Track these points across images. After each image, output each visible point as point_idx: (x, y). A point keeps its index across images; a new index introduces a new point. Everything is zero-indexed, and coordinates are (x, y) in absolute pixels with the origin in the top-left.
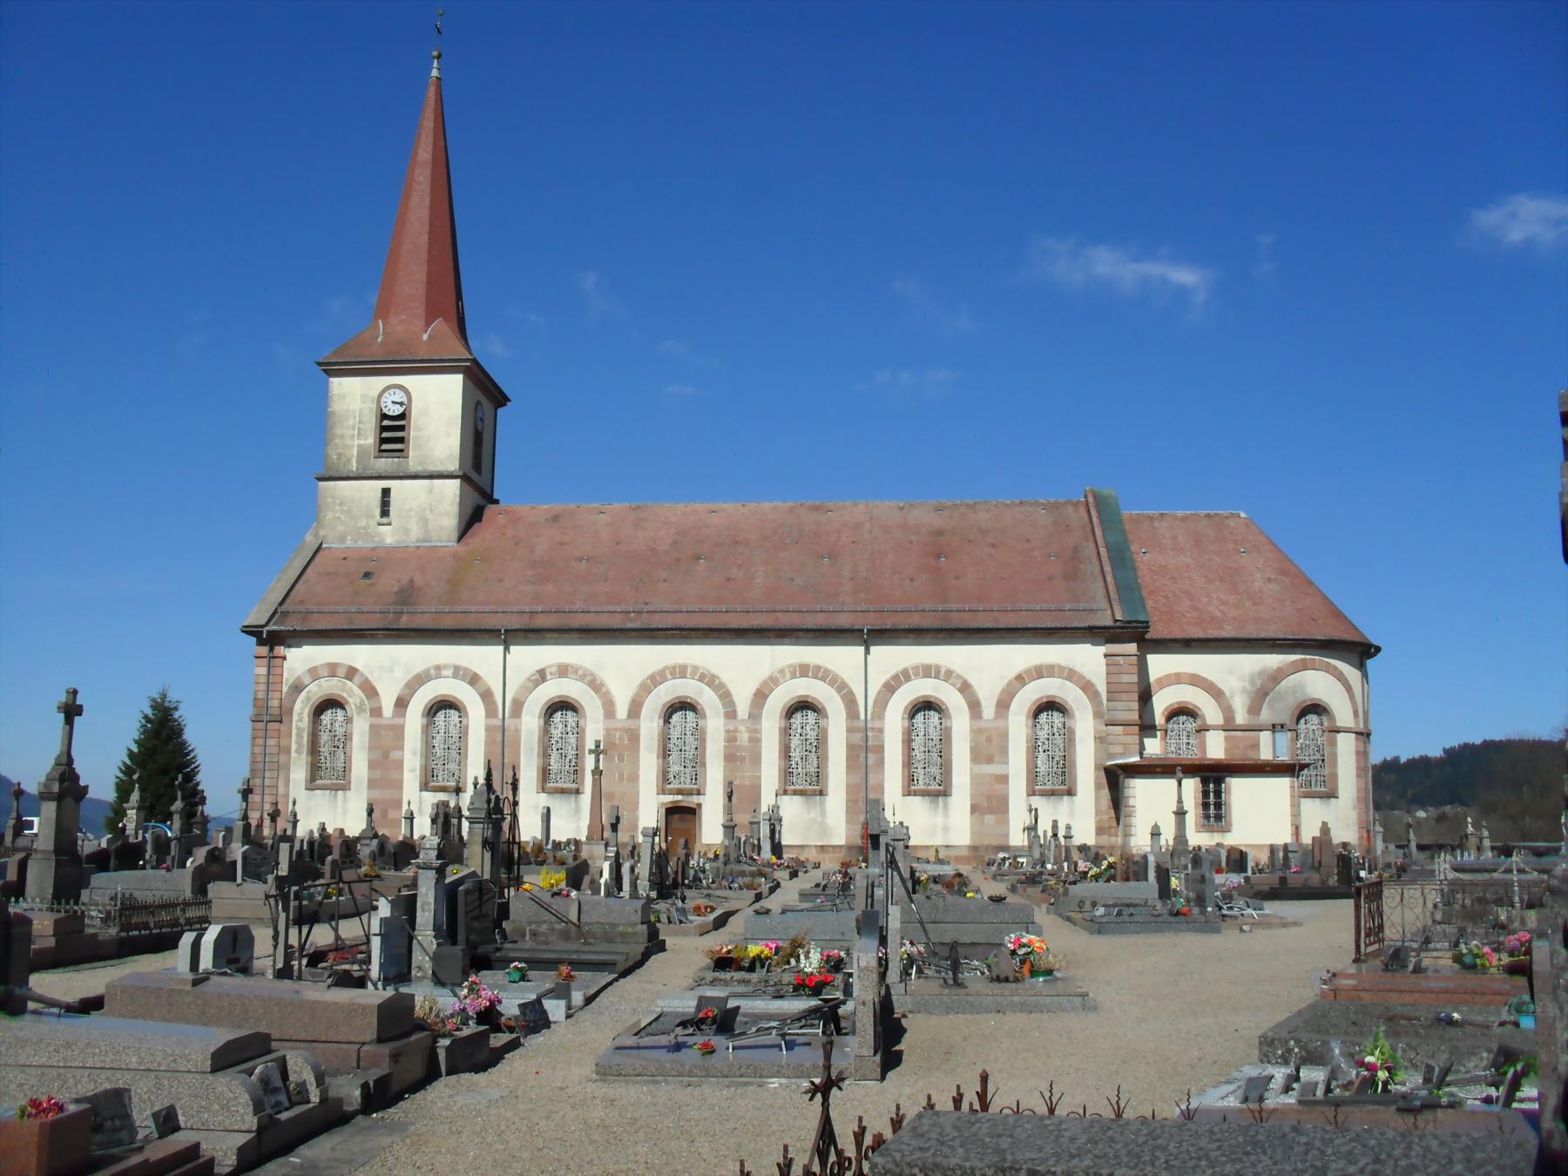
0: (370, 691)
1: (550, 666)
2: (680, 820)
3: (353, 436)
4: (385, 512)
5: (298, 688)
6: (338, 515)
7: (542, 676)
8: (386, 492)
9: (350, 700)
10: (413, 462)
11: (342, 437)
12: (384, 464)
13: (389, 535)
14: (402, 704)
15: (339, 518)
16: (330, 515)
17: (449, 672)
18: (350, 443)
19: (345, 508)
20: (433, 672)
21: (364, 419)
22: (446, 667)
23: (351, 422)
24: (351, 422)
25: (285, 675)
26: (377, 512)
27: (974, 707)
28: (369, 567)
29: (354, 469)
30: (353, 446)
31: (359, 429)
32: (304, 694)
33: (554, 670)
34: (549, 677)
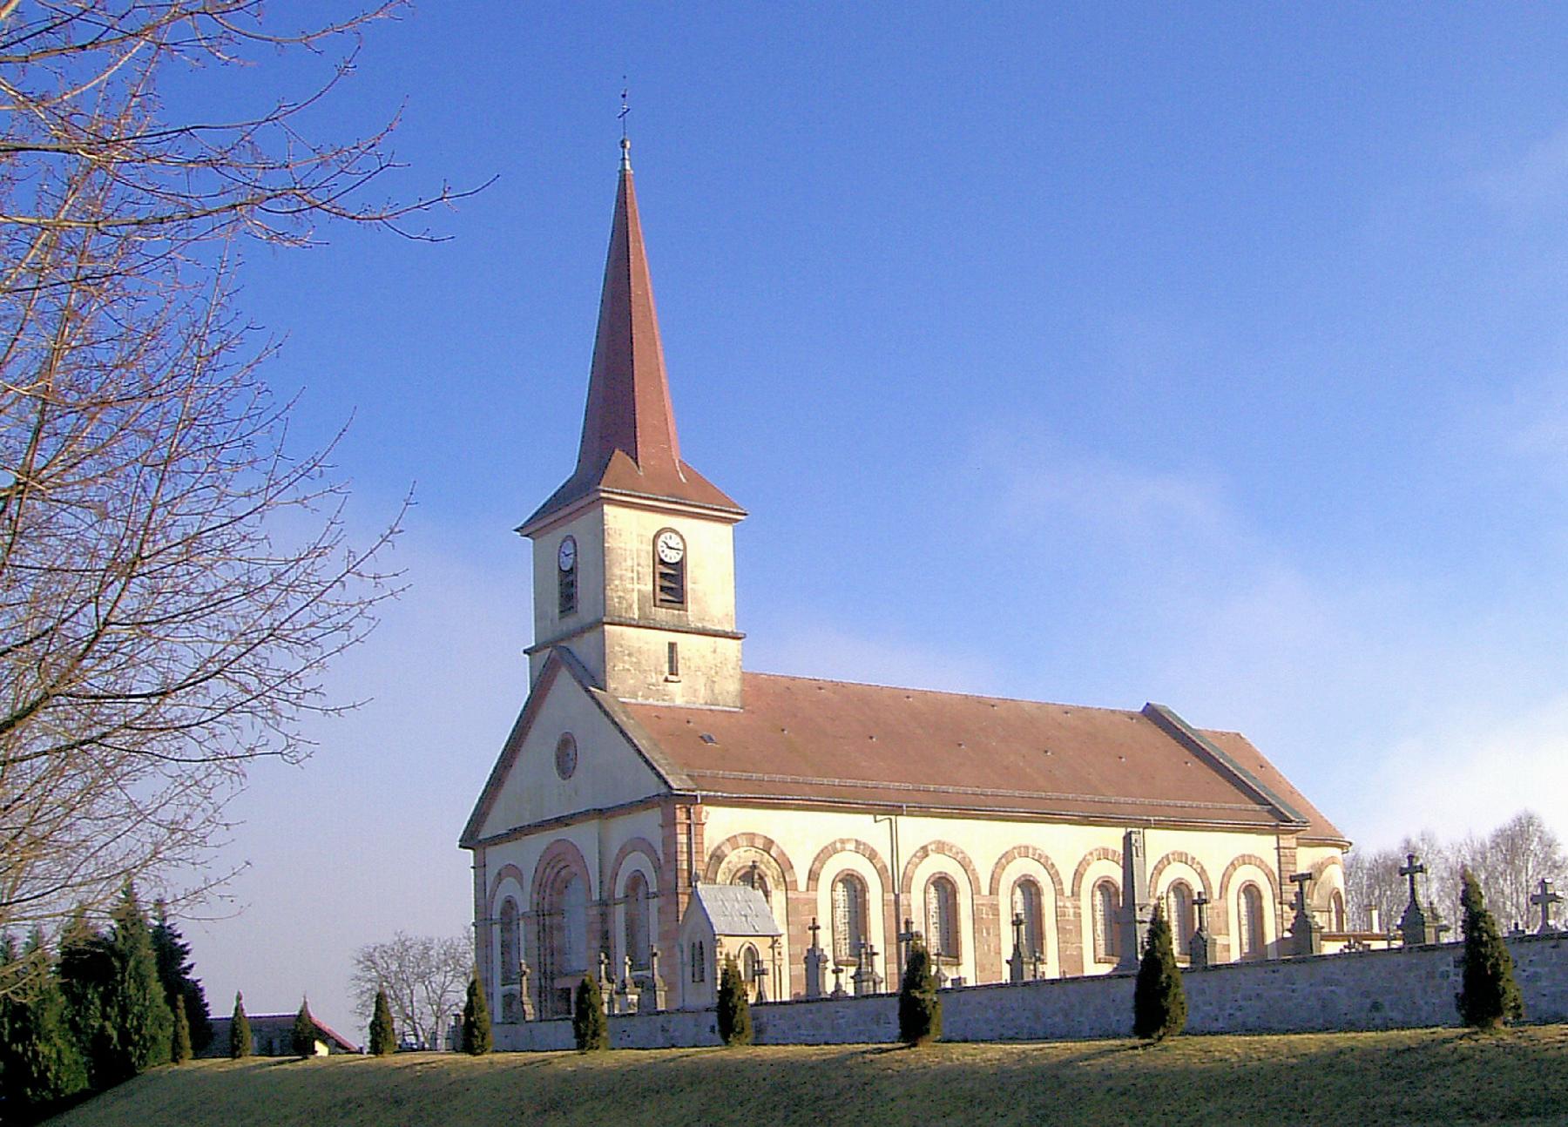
0: (785, 866)
1: (930, 844)
2: (799, 994)
3: (633, 579)
4: (673, 671)
5: (717, 857)
6: (627, 666)
7: (925, 851)
8: (672, 647)
9: (768, 872)
10: (693, 614)
11: (621, 578)
12: (662, 614)
13: (679, 695)
14: (813, 876)
15: (629, 670)
16: (620, 666)
17: (851, 846)
18: (629, 586)
19: (634, 660)
20: (838, 845)
21: (642, 563)
22: (848, 840)
23: (629, 563)
24: (629, 563)
25: (706, 844)
26: (666, 668)
27: (974, 882)
28: (1265, 765)
29: (636, 617)
30: (633, 590)
31: (638, 573)
32: (723, 865)
33: (933, 847)
34: (930, 852)
